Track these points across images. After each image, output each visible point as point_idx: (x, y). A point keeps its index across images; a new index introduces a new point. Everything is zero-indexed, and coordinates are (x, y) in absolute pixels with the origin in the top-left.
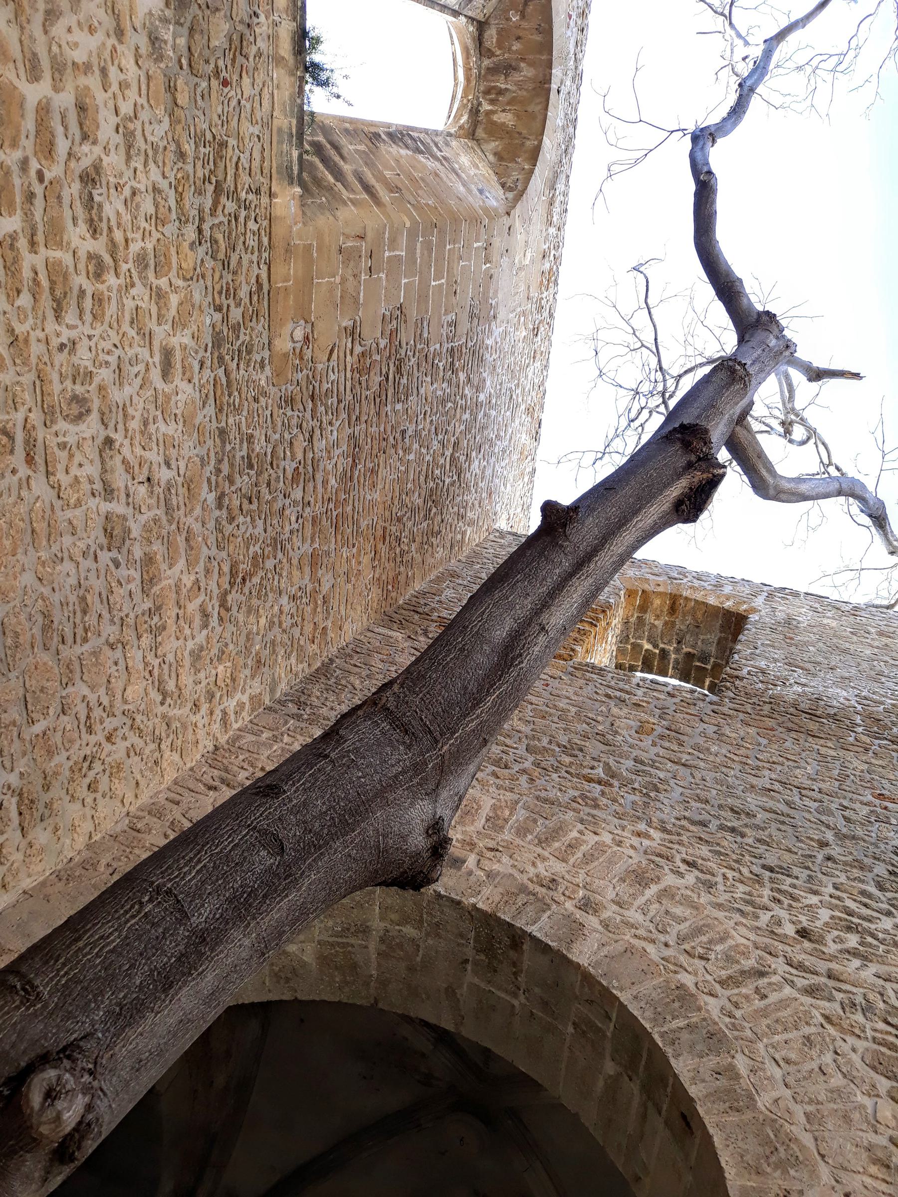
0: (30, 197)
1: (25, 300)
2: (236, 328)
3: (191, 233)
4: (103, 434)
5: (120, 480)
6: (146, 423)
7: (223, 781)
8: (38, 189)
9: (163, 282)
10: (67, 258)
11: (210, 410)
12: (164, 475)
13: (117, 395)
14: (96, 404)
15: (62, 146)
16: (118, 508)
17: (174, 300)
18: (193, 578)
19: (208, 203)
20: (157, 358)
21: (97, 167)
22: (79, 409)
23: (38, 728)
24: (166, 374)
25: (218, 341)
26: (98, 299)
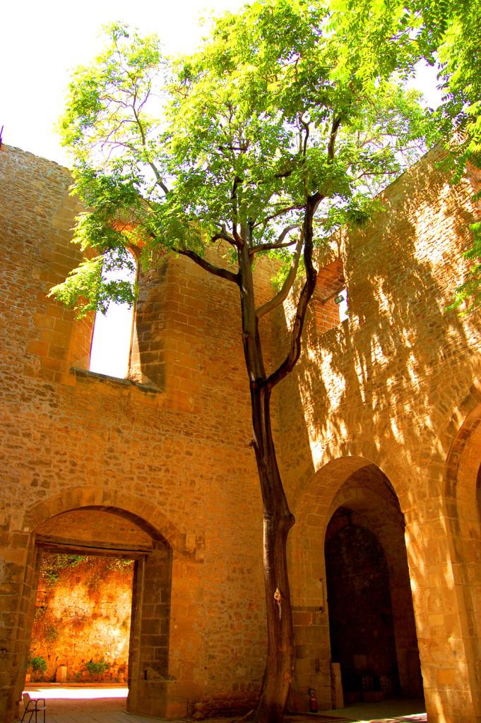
0: (153, 486)
1: (170, 492)
2: (186, 426)
3: (163, 438)
4: (199, 478)
5: (210, 475)
6: (200, 464)
7: (288, 466)
8: (152, 484)
9: (173, 451)
10: (164, 479)
11: (201, 440)
12: (212, 460)
13: (192, 471)
14: (193, 478)
15: (144, 475)
16: (215, 477)
17: (177, 448)
18: (237, 456)
19: (157, 431)
20: (187, 456)
21: (149, 466)
22: (193, 482)
23: (251, 511)
24: (191, 455)
25: (187, 434)
26: (173, 472)
